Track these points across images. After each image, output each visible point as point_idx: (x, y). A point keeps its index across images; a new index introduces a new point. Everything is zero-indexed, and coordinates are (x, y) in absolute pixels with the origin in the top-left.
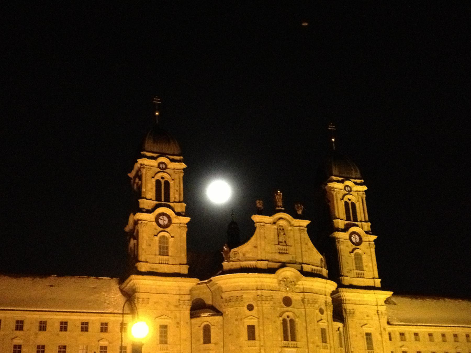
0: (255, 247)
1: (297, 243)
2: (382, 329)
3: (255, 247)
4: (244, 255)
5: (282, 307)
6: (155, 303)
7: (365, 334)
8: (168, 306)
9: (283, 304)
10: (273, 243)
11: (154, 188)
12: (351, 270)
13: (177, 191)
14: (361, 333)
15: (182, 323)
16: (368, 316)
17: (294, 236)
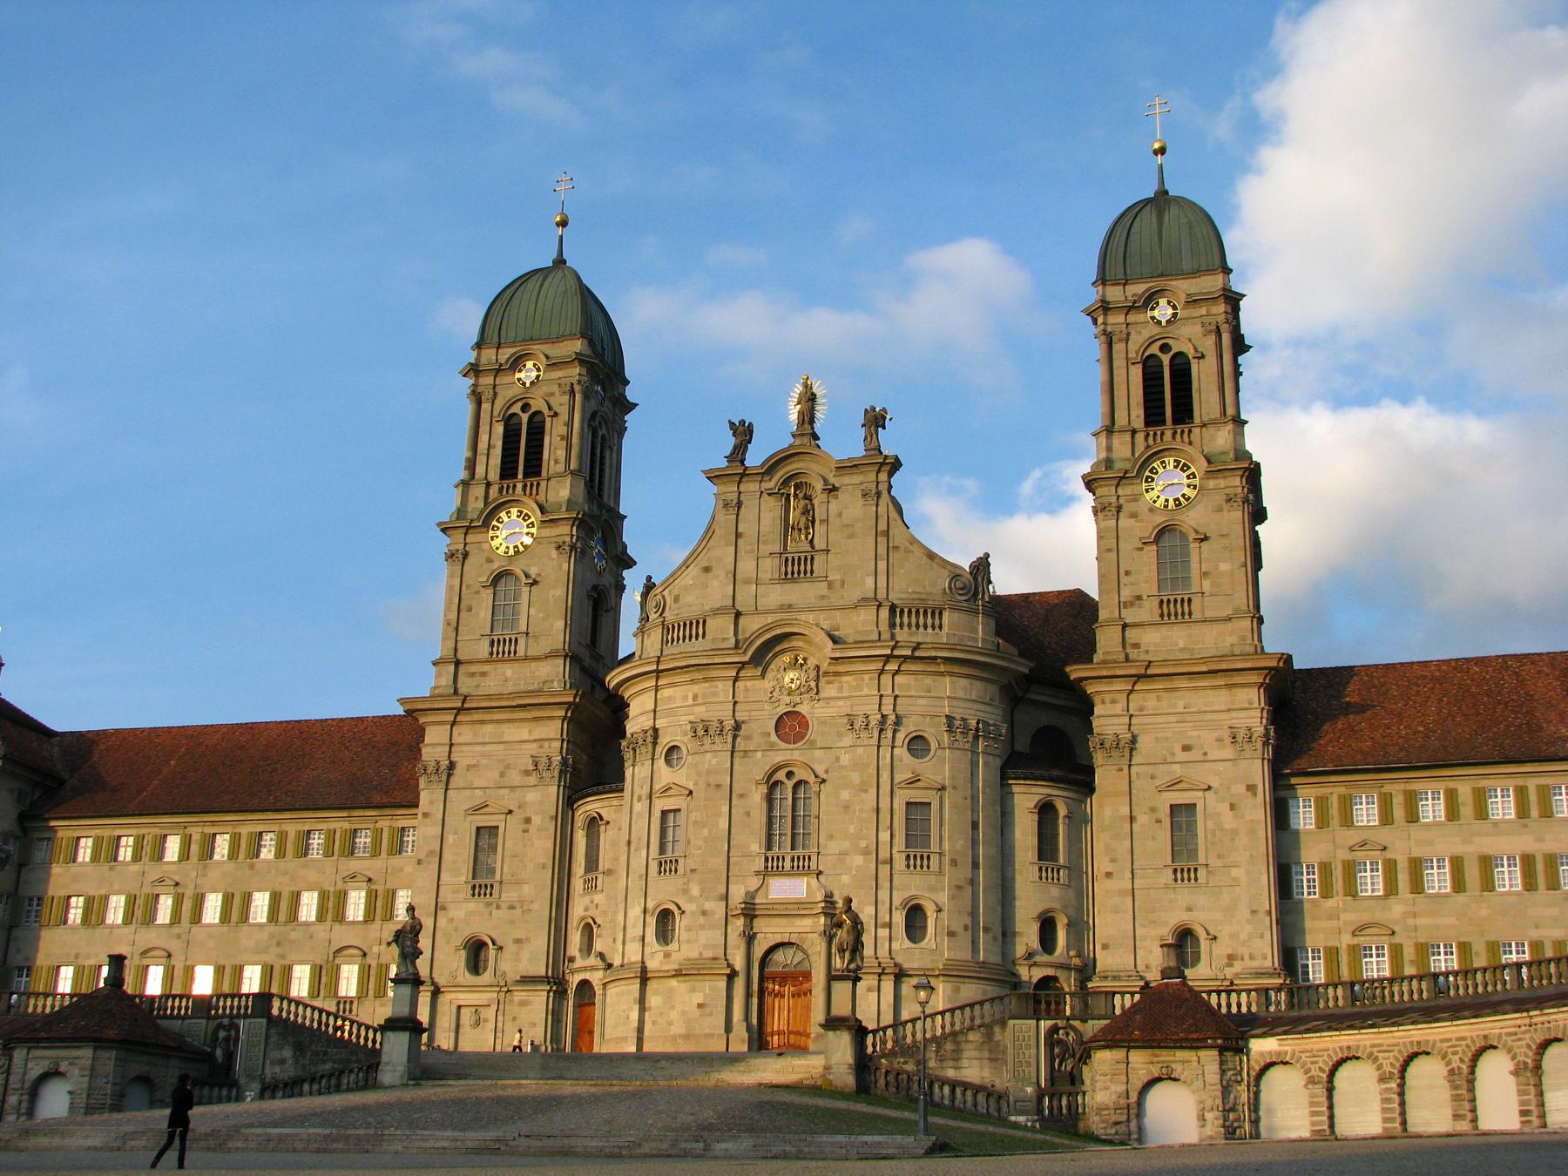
0: (707, 570)
1: (851, 536)
2: (1241, 789)
3: (707, 570)
4: (676, 599)
5: (772, 747)
6: (469, 767)
7: (1168, 810)
8: (502, 775)
9: (774, 738)
10: (765, 549)
11: (499, 444)
12: (1139, 598)
13: (562, 438)
14: (1153, 810)
15: (536, 820)
16: (1186, 748)
17: (840, 515)
